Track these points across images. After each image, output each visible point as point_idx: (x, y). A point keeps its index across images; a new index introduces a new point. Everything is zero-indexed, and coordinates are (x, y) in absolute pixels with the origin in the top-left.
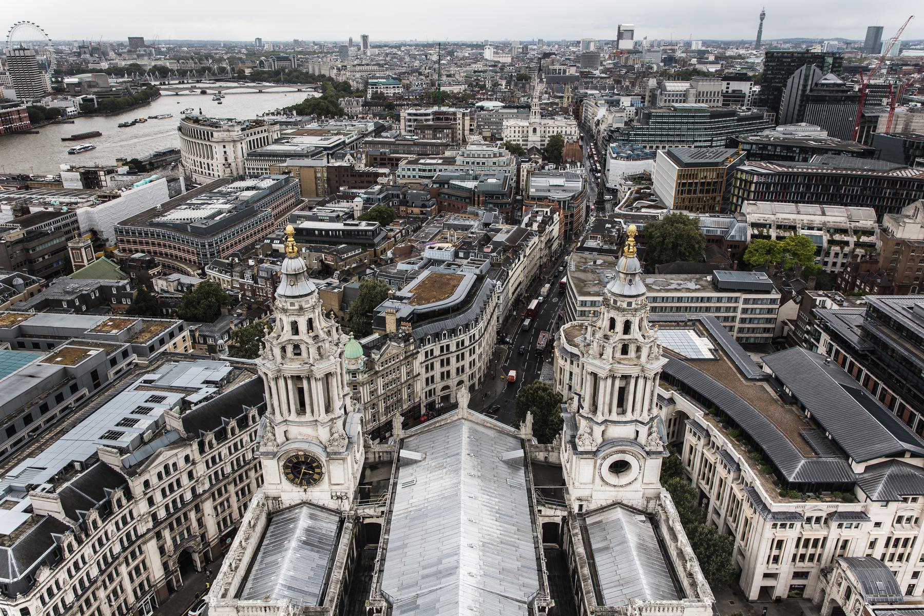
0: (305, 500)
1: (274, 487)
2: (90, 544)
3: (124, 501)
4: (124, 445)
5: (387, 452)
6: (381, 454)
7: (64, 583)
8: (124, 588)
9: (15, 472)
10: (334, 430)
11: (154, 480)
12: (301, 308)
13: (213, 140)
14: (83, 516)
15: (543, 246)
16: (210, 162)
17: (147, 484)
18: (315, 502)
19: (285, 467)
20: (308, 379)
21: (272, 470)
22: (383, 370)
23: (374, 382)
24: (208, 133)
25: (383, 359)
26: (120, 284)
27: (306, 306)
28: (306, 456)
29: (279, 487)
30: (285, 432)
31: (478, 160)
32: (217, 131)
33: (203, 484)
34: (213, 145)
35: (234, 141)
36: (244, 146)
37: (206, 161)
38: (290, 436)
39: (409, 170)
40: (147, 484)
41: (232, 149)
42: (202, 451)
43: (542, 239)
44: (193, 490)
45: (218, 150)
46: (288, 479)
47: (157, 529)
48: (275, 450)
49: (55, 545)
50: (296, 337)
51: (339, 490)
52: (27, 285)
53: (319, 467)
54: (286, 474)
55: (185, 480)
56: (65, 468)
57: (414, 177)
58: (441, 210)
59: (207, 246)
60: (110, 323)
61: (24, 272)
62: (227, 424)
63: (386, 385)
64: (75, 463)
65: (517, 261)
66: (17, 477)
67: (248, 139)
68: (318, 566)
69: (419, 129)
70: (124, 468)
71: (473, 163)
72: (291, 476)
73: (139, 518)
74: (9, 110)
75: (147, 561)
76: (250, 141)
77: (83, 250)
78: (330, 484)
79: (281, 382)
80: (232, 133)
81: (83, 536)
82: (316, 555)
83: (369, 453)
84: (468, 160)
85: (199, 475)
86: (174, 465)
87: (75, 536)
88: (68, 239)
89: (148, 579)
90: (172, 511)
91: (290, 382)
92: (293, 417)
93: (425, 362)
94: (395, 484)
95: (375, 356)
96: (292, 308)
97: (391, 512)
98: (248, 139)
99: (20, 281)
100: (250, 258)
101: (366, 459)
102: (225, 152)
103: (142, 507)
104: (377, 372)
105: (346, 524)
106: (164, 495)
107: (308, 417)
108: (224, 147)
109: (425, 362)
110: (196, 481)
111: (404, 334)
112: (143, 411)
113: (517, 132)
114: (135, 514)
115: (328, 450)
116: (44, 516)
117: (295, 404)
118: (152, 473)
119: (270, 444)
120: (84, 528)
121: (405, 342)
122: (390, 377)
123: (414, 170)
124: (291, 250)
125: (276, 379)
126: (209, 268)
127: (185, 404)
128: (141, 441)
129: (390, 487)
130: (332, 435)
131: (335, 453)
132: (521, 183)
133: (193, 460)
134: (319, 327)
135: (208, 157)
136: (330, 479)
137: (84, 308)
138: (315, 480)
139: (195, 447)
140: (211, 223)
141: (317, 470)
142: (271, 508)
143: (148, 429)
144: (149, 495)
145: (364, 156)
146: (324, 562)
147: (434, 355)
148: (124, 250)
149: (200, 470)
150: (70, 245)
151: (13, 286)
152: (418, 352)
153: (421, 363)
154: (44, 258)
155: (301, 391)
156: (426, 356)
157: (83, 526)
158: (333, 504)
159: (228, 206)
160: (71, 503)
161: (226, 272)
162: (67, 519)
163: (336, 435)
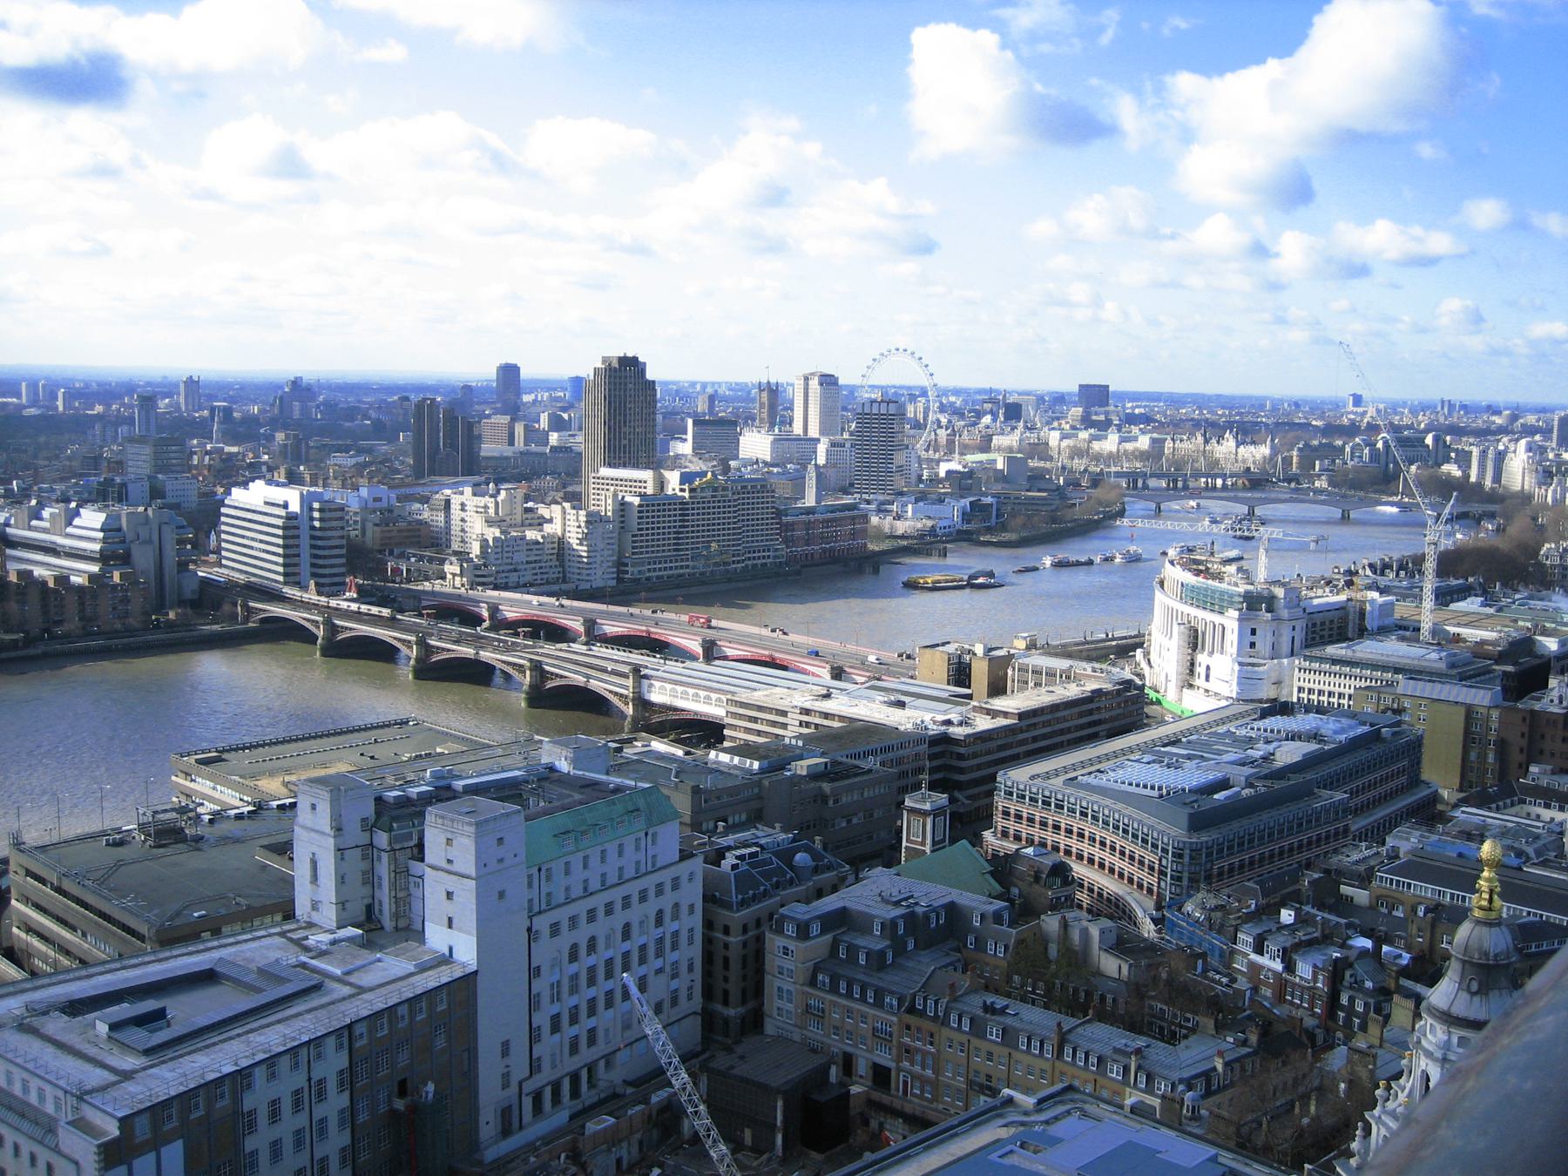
41: (1269, 639)
52: (816, 870)
74: (838, 514)
77: (929, 821)
88: (904, 790)
100: (1283, 904)
108: (1253, 632)
124: (1485, 903)
137: (911, 946)
140: (1205, 804)
148: (1005, 834)
150: (908, 803)
151: (792, 867)
154: (849, 821)
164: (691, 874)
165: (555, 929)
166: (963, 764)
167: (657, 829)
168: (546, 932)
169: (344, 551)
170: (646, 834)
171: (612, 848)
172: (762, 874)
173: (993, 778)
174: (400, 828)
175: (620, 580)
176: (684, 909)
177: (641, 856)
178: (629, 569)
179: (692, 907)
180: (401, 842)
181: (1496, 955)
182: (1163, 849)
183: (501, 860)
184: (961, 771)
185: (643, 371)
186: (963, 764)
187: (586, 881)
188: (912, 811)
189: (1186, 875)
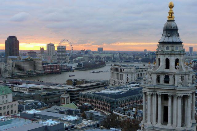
12: (173, 50)
13: (124, 72)
16: (121, 81)
24: (122, 69)
26: (77, 110)
27: (176, 50)
32: (126, 69)
34: (123, 74)
35: (132, 73)
36: (136, 75)
41: (131, 76)
45: (125, 76)
50: (167, 71)
59: (115, 103)
67: (138, 73)
76: (139, 74)
77: (66, 99)
80: (132, 70)
91: (160, 99)
92: (159, 125)
96: (167, 50)
98: (138, 73)
102: (128, 77)
108: (128, 75)
125: (152, 95)
126: (115, 111)
134: (182, 66)
154: (51, 104)
155: (165, 109)
166: (74, 93)
167: (8, 95)
170: (5, 95)
172: (31, 106)
173: (78, 93)
175: (12, 76)
176: (14, 112)
177: (4, 100)
178: (14, 74)
179: (15, 112)
181: (174, 27)
182: (111, 102)
184: (73, 97)
185: (16, 39)
186: (74, 96)
188: (62, 98)
189: (115, 106)
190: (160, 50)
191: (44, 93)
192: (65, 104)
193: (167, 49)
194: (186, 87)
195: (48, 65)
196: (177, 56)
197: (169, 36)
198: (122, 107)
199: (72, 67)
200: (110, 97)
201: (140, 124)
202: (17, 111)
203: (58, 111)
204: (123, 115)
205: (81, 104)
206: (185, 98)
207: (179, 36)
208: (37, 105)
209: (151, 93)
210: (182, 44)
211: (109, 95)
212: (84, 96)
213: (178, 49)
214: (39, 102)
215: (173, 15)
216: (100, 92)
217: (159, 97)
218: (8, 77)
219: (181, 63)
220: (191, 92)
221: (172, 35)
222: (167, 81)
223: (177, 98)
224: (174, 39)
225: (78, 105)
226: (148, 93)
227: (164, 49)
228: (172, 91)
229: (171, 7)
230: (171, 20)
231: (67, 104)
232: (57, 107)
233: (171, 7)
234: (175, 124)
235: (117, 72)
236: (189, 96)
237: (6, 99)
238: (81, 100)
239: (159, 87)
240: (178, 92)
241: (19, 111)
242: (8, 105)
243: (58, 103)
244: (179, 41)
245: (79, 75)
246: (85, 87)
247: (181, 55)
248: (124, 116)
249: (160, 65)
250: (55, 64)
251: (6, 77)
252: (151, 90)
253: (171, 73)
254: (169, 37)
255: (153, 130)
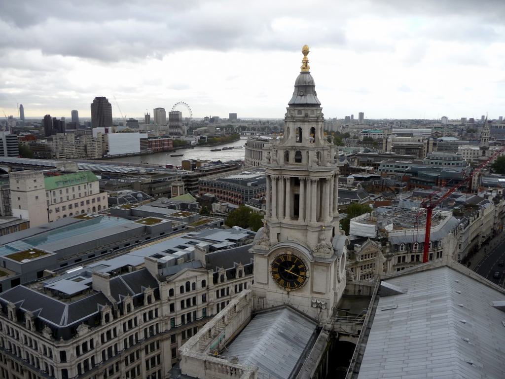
0: (286, 302)
1: (261, 286)
2: (122, 322)
3: (153, 299)
4: (163, 262)
5: (367, 287)
6: (361, 288)
7: (97, 345)
8: (140, 372)
9: (92, 265)
10: (322, 237)
11: (177, 291)
12: (306, 116)
14: (122, 298)
15: (497, 215)
16: (260, 161)
17: (171, 292)
18: (296, 307)
19: (274, 266)
20: (305, 182)
21: (262, 267)
22: (362, 262)
23: (354, 270)
24: (261, 144)
25: (363, 253)
28: (294, 257)
29: (266, 287)
30: (278, 234)
31: (440, 161)
32: (267, 143)
33: (212, 309)
37: (257, 161)
38: (282, 238)
39: (388, 166)
40: (171, 292)
42: (215, 281)
43: (497, 209)
44: (204, 312)
45: (265, 154)
46: (274, 278)
47: (172, 333)
48: (267, 248)
49: (97, 312)
50: (299, 144)
51: (318, 299)
52: (143, 199)
53: (304, 270)
54: (274, 273)
55: (199, 300)
56: (122, 268)
57: (391, 171)
58: (410, 188)
59: (249, 193)
60: (180, 213)
61: (145, 192)
62: (237, 266)
63: (363, 277)
64: (130, 267)
65: (476, 216)
66: (92, 268)
68: (290, 356)
69: (396, 148)
70: (158, 276)
71: (436, 163)
72: (277, 276)
73: (161, 318)
75: (161, 357)
77: (179, 187)
78: (313, 292)
79: (281, 183)
81: (118, 313)
82: (290, 348)
83: (349, 286)
84: (432, 161)
85: (210, 300)
86: (194, 284)
87: (113, 309)
89: (159, 371)
90: (186, 322)
91: (288, 184)
92: (287, 220)
93: (397, 265)
94: (374, 310)
95: (358, 248)
97: (369, 328)
99: (140, 195)
101: (346, 290)
103: (165, 310)
104: (357, 263)
105: (322, 334)
106: (182, 307)
107: (300, 221)
109: (397, 265)
110: (208, 305)
111: (382, 237)
112: (182, 248)
113: (469, 154)
114: (159, 314)
115: (315, 255)
116: (97, 292)
117: (290, 207)
118: (177, 285)
119: (263, 243)
120: (121, 307)
121: (382, 245)
122: (367, 270)
123: (391, 166)
125: (278, 179)
127: (211, 249)
128: (175, 262)
129: (369, 311)
130: (319, 240)
131: (321, 258)
132: (472, 185)
133: (208, 286)
134: (320, 138)
135: (259, 160)
136: (312, 287)
138: (298, 283)
139: (211, 276)
141: (302, 273)
142: (256, 305)
143: (182, 256)
144: (171, 302)
145: (356, 160)
146: (298, 356)
147: (406, 261)
149: (212, 297)
152: (392, 256)
153: (394, 266)
155: (296, 198)
156: (399, 261)
157: (120, 306)
158: (312, 312)
159: (264, 174)
160: (116, 288)
161: (258, 206)
162: (111, 297)
163: (323, 242)
164: (104, 197)
165: (58, 210)
167: (92, 183)
168: (54, 211)
169: (18, 149)
171: (76, 188)
172: (128, 199)
173: (197, 180)
174: (4, 183)
176: (102, 208)
177: (86, 191)
179: (104, 207)
180: (6, 188)
181: (308, 82)
183: (36, 187)
187: (68, 196)
188: (173, 187)
190: (289, 116)
191: (148, 180)
192: (177, 195)
193: (298, 114)
194: (323, 167)
195: (156, 139)
196: (312, 123)
197: (302, 95)
198: (258, 197)
199: (191, 143)
200: (242, 184)
201: (263, 220)
202: (107, 206)
203: (166, 206)
204: (259, 209)
205: (201, 195)
206: (322, 182)
207: (316, 95)
208: (137, 198)
209: (277, 176)
210: (321, 106)
211: (240, 182)
212: (205, 183)
213: (314, 114)
214: (138, 193)
215: (308, 64)
216: (226, 178)
217: (287, 181)
218: (96, 158)
219: (319, 134)
220: (333, 173)
221: (307, 94)
222: (299, 160)
223: (312, 182)
224: (309, 100)
225: (197, 196)
226: (272, 176)
227: (296, 113)
228: (304, 174)
229: (306, 52)
230: (305, 71)
231: (180, 195)
232: (166, 200)
233: (306, 52)
234: (309, 218)
235: (254, 148)
236: (327, 179)
237: (90, 190)
238: (201, 189)
239: (288, 167)
240: (312, 174)
241: (109, 206)
242: (88, 199)
243: (168, 194)
244: (316, 103)
245: (191, 155)
246: (207, 171)
247: (318, 122)
248: (261, 211)
249: (290, 137)
250: (167, 139)
251: (94, 158)
252: (275, 172)
253: (304, 148)
254: (301, 96)
255: (278, 227)
